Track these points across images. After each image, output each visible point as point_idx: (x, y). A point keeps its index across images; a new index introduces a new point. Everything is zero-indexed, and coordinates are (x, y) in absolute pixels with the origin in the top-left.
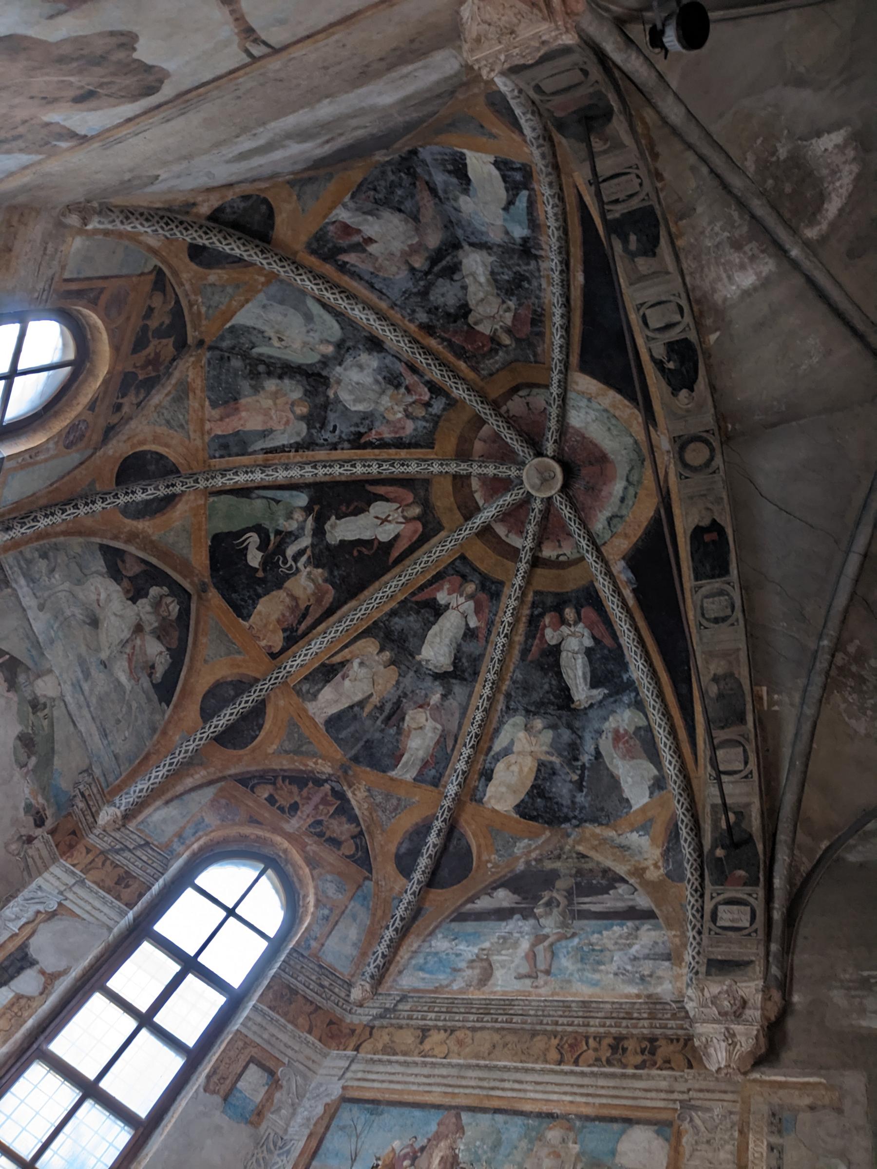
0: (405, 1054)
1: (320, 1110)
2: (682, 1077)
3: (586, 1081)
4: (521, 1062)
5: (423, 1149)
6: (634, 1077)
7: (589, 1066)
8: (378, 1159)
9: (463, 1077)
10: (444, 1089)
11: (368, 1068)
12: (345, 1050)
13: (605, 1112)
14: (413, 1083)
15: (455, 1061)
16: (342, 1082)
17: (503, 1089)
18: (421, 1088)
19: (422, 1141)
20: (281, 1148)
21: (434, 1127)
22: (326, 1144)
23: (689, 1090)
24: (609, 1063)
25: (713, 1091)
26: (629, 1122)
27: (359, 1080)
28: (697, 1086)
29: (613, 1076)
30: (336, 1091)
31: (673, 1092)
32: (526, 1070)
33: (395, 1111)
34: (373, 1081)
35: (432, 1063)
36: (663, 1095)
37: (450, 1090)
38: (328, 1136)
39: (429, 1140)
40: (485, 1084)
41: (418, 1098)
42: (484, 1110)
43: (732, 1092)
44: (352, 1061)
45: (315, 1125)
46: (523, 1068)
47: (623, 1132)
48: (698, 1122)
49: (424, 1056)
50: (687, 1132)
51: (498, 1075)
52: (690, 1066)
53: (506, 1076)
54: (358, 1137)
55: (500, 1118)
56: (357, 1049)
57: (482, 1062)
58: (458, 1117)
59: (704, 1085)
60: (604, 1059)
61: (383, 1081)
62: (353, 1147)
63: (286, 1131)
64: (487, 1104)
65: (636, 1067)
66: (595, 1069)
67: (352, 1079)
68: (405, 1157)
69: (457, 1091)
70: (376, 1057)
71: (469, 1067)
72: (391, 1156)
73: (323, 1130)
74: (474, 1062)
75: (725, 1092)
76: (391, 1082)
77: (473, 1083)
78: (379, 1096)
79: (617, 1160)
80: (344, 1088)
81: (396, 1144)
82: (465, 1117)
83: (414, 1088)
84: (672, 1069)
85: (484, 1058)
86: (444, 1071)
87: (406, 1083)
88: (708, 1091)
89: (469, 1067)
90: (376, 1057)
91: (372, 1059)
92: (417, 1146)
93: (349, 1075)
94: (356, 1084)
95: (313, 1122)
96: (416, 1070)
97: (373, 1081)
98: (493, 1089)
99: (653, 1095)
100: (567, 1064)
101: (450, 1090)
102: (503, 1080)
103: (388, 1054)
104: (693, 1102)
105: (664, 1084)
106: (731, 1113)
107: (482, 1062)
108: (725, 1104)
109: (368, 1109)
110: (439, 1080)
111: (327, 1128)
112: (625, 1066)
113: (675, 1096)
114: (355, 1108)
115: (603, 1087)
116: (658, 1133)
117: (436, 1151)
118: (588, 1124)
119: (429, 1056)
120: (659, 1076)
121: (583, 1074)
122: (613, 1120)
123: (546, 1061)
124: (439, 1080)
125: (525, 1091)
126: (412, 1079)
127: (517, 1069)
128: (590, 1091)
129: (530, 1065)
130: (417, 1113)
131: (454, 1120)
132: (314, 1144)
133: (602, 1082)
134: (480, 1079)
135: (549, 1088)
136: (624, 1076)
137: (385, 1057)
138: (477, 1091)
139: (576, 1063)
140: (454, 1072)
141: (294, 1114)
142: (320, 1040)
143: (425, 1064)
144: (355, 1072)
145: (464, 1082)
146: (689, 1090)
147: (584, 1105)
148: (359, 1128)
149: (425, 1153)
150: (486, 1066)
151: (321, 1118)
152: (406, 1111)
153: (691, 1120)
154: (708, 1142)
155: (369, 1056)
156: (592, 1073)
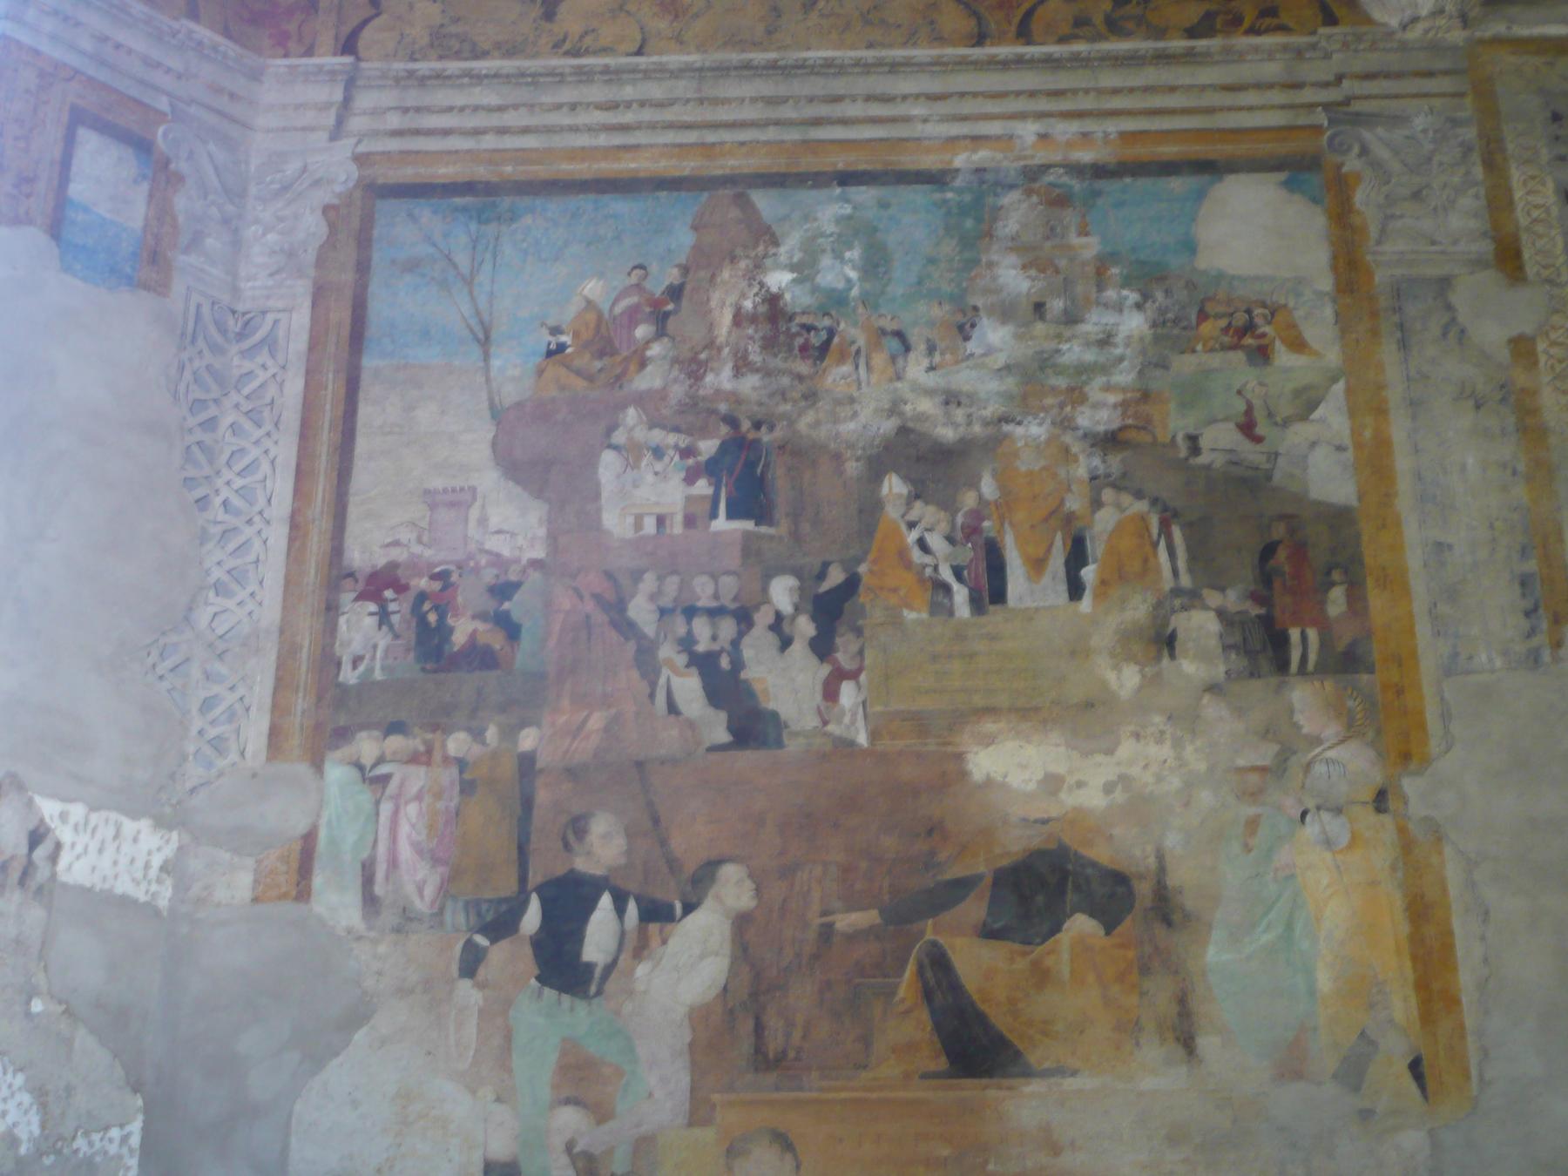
0: (511, 51)
1: (312, 226)
2: (1314, 47)
3: (1063, 80)
4: (870, 46)
5: (675, 293)
6: (1190, 57)
7: (1062, 40)
8: (556, 331)
9: (717, 102)
10: (671, 137)
11: (413, 97)
12: (309, 52)
13: (1142, 152)
14: (574, 129)
15: (675, 59)
16: (346, 147)
17: (844, 122)
18: (603, 140)
19: (663, 277)
20: (241, 336)
21: (683, 239)
22: (380, 308)
23: (1339, 79)
24: (1114, 27)
25: (1399, 75)
26: (1210, 168)
27: (398, 133)
28: (1358, 66)
29: (1132, 60)
30: (337, 168)
31: (1297, 86)
32: (894, 67)
33: (554, 206)
34: (446, 132)
35: (606, 70)
36: (1278, 97)
37: (691, 137)
38: (376, 288)
39: (685, 270)
40: (787, 112)
41: (606, 167)
42: (818, 180)
43: (1446, 73)
44: (350, 85)
45: (320, 263)
46: (880, 63)
47: (1201, 195)
48: (1383, 153)
49: (575, 53)
50: (1358, 177)
51: (817, 86)
52: (1331, 20)
53: (838, 86)
54: (469, 282)
55: (865, 195)
56: (349, 46)
57: (759, 57)
58: (742, 201)
59: (1372, 61)
60: (1098, 19)
61: (477, 132)
62: (466, 308)
63: (235, 291)
64: (808, 163)
65: (1191, 33)
66: (1080, 47)
67: (375, 134)
68: (632, 317)
69: (711, 137)
70: (423, 67)
71: (722, 71)
72: (591, 317)
73: (348, 277)
74: (735, 57)
75: (1430, 74)
76: (502, 131)
77: (749, 113)
78: (481, 172)
79: (1203, 262)
80: (361, 159)
81: (592, 288)
82: (765, 202)
83: (583, 140)
84: (1283, 29)
85: (756, 45)
86: (656, 91)
87: (549, 130)
88: (1387, 75)
89: (722, 71)
90: (423, 67)
91: (411, 74)
92: (657, 287)
93: (356, 123)
94: (394, 145)
95: (310, 256)
96: (567, 95)
97: (446, 132)
98: (817, 122)
99: (1250, 98)
100: (1000, 39)
101: (691, 137)
102: (837, 99)
103: (457, 55)
104: (1357, 106)
105: (1271, 70)
106: (1455, 123)
107: (759, 57)
108: (1437, 102)
109: (465, 209)
110: (647, 115)
111: (363, 268)
112: (1160, 33)
113: (1308, 95)
114: (425, 212)
115: (1116, 91)
116: (1289, 185)
117: (716, 297)
118: (1101, 184)
119: (587, 52)
120: (1256, 49)
121: (1051, 63)
122: (1168, 168)
123: (939, 39)
124: (647, 115)
125: (907, 119)
126: (564, 119)
127: (866, 68)
128: (1087, 103)
129: (899, 53)
130: (619, 206)
131: (734, 213)
132: (340, 314)
133: (1109, 79)
134: (771, 101)
135: (968, 107)
136: (1163, 58)
137: (453, 66)
138: (771, 134)
139: (1024, 34)
140: (682, 88)
141: (236, 244)
142: (227, 33)
143: (585, 76)
144: (376, 112)
145: (724, 114)
146: (1339, 79)
147: (1098, 142)
148: (463, 260)
149: (685, 303)
150: (773, 66)
151: (330, 244)
152: (585, 202)
153: (1364, 151)
154: (1416, 196)
155: (399, 66)
156: (1076, 58)
